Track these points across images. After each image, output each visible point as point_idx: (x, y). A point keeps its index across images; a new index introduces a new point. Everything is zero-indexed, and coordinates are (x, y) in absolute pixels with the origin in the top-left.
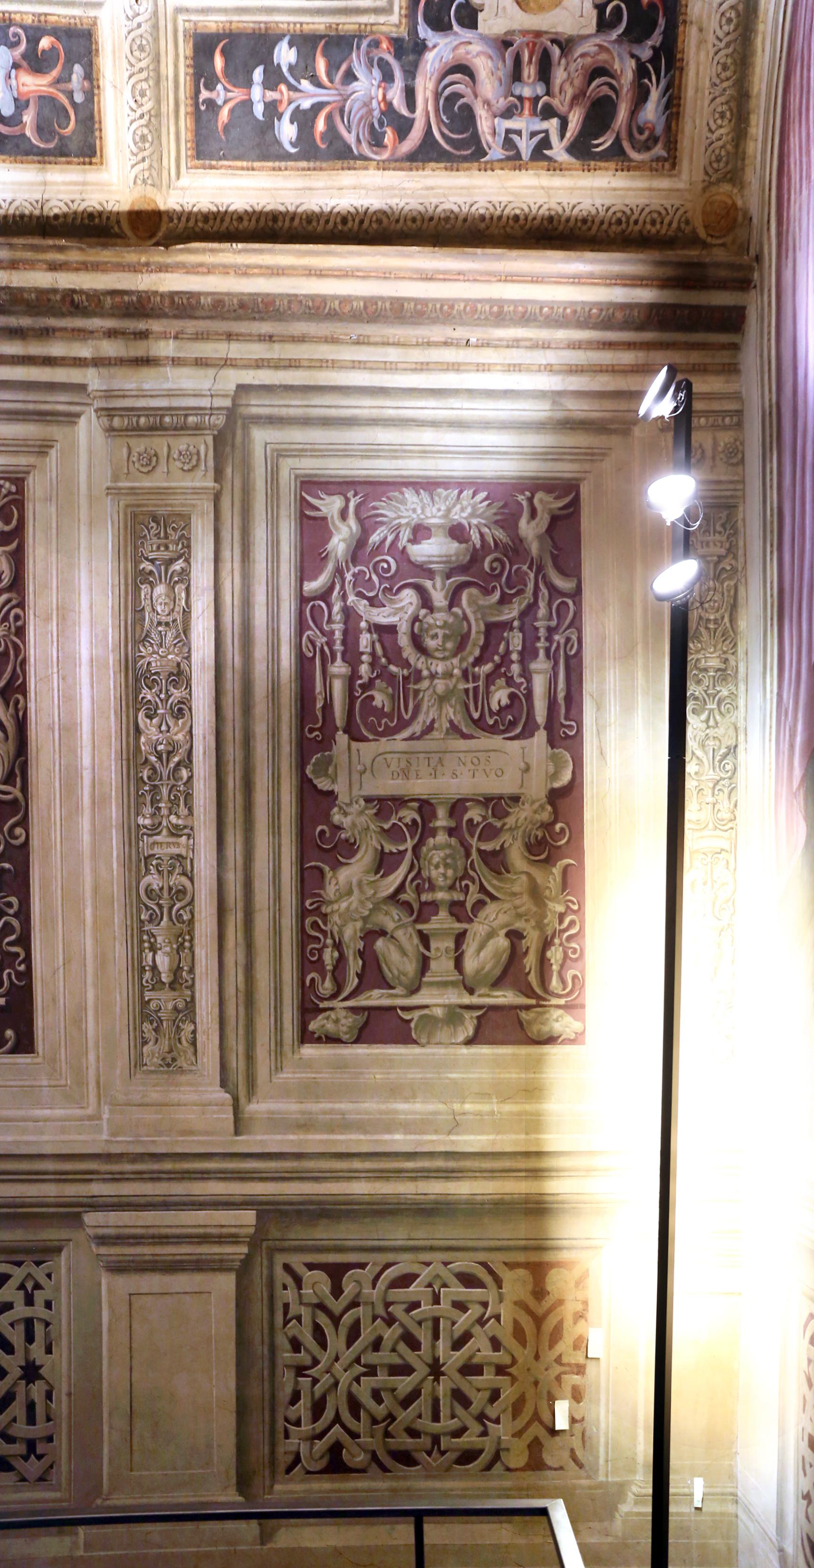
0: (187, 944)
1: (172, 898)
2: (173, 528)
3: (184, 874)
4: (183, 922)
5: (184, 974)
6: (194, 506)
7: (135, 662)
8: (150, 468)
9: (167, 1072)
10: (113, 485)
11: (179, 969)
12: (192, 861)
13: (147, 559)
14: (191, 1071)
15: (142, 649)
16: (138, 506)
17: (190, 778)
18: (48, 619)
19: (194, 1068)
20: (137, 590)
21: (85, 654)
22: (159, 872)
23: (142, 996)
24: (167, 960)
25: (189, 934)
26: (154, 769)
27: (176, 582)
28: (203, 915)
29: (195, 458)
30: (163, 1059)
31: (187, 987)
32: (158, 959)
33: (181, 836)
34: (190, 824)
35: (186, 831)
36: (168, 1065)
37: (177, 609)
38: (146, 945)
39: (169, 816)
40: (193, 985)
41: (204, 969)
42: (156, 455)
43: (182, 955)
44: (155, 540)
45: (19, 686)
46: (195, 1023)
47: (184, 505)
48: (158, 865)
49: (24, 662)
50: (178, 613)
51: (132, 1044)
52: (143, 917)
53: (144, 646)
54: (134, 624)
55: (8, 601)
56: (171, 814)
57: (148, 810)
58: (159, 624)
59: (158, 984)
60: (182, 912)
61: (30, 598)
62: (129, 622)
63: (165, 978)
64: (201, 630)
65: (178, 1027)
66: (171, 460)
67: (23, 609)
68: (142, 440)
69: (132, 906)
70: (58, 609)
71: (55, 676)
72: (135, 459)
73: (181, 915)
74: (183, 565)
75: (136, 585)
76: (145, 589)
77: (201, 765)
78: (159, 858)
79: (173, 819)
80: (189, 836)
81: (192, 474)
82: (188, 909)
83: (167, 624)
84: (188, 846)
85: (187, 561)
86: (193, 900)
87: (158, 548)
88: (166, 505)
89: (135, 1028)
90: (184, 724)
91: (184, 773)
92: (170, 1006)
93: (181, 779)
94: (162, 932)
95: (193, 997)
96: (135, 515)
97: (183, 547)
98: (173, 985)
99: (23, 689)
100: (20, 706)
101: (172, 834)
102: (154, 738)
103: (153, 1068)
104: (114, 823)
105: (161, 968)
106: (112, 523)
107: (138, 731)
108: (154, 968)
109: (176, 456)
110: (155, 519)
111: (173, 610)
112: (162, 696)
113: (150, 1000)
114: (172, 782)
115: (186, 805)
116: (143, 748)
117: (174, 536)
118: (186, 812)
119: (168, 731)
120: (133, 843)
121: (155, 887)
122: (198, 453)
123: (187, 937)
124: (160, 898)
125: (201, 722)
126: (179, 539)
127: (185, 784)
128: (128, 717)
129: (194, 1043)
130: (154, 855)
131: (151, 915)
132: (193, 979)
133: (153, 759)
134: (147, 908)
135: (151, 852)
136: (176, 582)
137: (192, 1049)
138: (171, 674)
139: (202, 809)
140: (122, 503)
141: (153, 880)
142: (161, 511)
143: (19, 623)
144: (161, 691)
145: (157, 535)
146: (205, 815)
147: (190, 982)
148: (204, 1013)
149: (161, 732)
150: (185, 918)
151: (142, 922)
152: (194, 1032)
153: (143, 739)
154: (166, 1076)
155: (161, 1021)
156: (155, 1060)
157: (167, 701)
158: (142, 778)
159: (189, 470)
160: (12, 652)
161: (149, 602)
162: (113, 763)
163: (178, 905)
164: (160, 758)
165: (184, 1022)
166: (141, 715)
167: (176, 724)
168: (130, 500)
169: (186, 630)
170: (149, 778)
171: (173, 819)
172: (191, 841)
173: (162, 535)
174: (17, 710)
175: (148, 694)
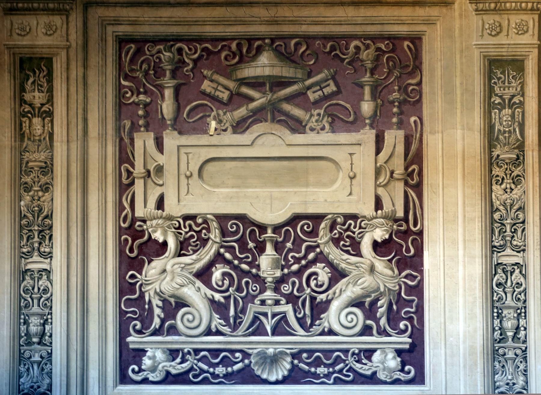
0: (523, 314)
60: (519, 296)
153: (493, 194)
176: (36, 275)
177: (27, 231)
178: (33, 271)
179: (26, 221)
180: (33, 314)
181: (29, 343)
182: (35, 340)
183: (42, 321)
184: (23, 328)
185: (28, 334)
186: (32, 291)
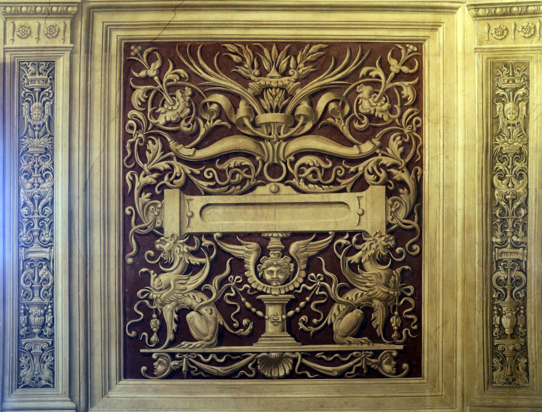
0: (522, 311)
1: (512, 285)
2: (518, 70)
3: (521, 270)
4: (520, 298)
5: (520, 329)
6: (531, 57)
7: (492, 147)
8: (503, 37)
9: (509, 387)
10: (479, 47)
11: (517, 326)
12: (526, 262)
13: (501, 88)
14: (525, 386)
15: (497, 140)
16: (495, 58)
17: (526, 214)
18: (437, 123)
19: (527, 385)
20: (494, 106)
21: (460, 142)
22: (505, 269)
23: (493, 342)
24: (509, 321)
25: (523, 306)
26: (503, 209)
27: (519, 101)
28: (533, 294)
29: (533, 30)
30: (507, 380)
31: (522, 337)
32: (503, 320)
33: (519, 248)
34: (525, 241)
35: (522, 245)
36: (510, 383)
37: (520, 116)
38: (496, 312)
39: (512, 237)
40: (526, 335)
41: (533, 327)
42: (507, 29)
43: (519, 318)
44: (506, 77)
45: (418, 162)
46: (527, 358)
47: (524, 57)
48: (504, 265)
49: (421, 148)
50: (521, 118)
51: (486, 371)
52: (494, 296)
53: (499, 138)
54: (492, 126)
55: (412, 113)
56: (513, 235)
57: (499, 233)
58: (509, 125)
59: (502, 335)
60: (519, 293)
61: (426, 111)
62: (489, 124)
63: (507, 331)
64: (535, 128)
65: (517, 360)
66: (517, 32)
67: (422, 117)
68: (498, 21)
69: (487, 290)
70: (443, 117)
71: (442, 156)
72: (493, 32)
73: (518, 295)
74: (524, 91)
75: (493, 102)
76: (499, 105)
77: (534, 207)
78: (505, 261)
79: (515, 238)
80: (524, 248)
81: (531, 39)
82: (523, 291)
83: (514, 125)
84: (523, 254)
85: (527, 89)
86: (526, 285)
87: (508, 82)
88: (513, 57)
89: (488, 361)
90: (523, 183)
91: (523, 211)
92: (511, 348)
93: (521, 215)
94: (506, 306)
95: (526, 343)
96: (493, 63)
97: (524, 81)
98: (512, 336)
99: (421, 164)
100: (418, 173)
101: (513, 247)
102: (504, 191)
103: (500, 385)
104: (477, 241)
105: (505, 326)
106: (478, 68)
107: (493, 187)
108: (501, 326)
109: (520, 30)
110: (506, 65)
111: (518, 117)
112: (509, 167)
113: (497, 345)
114: (515, 217)
115: (523, 230)
116: (497, 197)
117: (518, 75)
118: (523, 234)
119: (513, 187)
120: (489, 253)
121: (502, 278)
122: (535, 27)
123: (522, 307)
124: (505, 285)
125: (534, 182)
126: (522, 76)
127: (522, 218)
128: (486, 179)
129: (527, 370)
130: (502, 259)
131: (499, 295)
132: (526, 332)
133: (503, 203)
134: (497, 291)
135: (500, 258)
136: (519, 101)
137: (526, 374)
138: (516, 154)
139: (533, 232)
140: (484, 57)
141: (501, 274)
142: (510, 61)
143: (419, 125)
144: (508, 164)
145: (508, 74)
146: (535, 236)
147: (524, 334)
148: (533, 352)
149: (509, 188)
150: (521, 296)
151: (493, 299)
152: (527, 363)
153: (496, 192)
154: (508, 390)
155: (505, 357)
156: (501, 380)
157: (512, 169)
158: (495, 214)
159: (529, 37)
160: (414, 142)
161: (502, 113)
162: (477, 206)
163: (517, 289)
164: (507, 202)
165: (520, 357)
166: (495, 178)
167: (518, 183)
168: (490, 55)
169: (526, 129)
170: (500, 215)
171: (515, 238)
172: (526, 251)
173: (511, 74)
174: (416, 176)
175: (500, 166)
176: (36, 265)
177: (27, 220)
178: (33, 261)
179: (26, 209)
180: (34, 304)
181: (30, 334)
182: (36, 331)
183: (42, 311)
184: (23, 318)
185: (28, 324)
186: (32, 281)
